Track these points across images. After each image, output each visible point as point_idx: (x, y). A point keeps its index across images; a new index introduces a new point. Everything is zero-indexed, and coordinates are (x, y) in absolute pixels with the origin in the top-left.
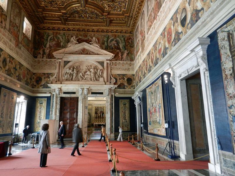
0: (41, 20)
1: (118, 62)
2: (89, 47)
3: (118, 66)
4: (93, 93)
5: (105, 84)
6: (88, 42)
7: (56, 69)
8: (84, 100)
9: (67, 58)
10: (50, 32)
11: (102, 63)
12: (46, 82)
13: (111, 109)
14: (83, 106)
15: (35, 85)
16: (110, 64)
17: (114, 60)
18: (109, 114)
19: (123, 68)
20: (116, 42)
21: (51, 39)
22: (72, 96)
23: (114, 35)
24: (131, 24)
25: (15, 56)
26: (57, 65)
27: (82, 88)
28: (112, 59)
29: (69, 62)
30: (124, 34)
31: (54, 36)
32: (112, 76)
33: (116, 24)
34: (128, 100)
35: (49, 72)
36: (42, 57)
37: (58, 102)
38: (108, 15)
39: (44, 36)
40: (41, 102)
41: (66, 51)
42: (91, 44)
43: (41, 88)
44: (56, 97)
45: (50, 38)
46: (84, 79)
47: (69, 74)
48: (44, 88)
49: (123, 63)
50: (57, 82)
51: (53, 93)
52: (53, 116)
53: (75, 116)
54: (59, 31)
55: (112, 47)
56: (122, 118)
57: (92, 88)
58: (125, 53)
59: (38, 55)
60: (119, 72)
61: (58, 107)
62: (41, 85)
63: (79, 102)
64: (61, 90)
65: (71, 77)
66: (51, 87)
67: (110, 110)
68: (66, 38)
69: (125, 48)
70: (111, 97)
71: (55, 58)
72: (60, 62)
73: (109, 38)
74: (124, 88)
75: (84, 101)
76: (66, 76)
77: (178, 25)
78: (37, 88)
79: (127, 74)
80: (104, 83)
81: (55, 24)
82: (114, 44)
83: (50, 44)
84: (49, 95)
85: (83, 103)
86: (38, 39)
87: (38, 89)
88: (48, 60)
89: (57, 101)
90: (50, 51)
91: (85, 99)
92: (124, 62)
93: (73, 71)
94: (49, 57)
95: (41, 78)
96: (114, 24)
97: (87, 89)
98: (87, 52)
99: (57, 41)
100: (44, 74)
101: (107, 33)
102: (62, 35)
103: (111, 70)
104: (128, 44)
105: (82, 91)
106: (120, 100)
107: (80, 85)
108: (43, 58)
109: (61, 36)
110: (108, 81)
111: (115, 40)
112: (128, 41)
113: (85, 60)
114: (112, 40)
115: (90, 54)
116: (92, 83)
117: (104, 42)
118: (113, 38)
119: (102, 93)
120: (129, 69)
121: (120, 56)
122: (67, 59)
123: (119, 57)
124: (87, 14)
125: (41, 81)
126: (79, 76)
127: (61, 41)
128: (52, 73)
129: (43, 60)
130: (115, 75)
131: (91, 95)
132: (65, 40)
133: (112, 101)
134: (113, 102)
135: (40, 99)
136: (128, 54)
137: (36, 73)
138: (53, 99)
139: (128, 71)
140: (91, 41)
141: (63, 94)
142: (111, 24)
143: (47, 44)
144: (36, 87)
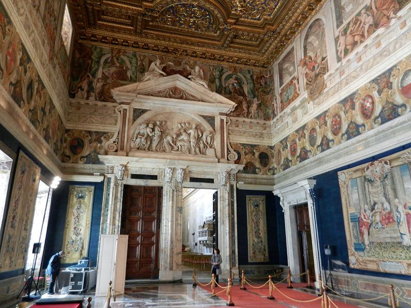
0: (92, 18)
1: (241, 119)
2: (187, 85)
3: (241, 129)
4: (193, 180)
5: (219, 162)
6: (186, 75)
7: (116, 124)
8: (175, 193)
9: (140, 102)
10: (106, 47)
11: (210, 120)
13: (231, 214)
14: (172, 207)
15: (69, 157)
16: (227, 123)
18: (227, 226)
19: (251, 132)
20: (236, 81)
21: (106, 62)
24: (270, 49)
29: (144, 111)
31: (112, 57)
32: (231, 147)
33: (240, 46)
34: (263, 197)
35: (101, 128)
36: (85, 96)
37: (119, 195)
38: (235, 24)
39: (92, 53)
40: (80, 195)
42: (189, 79)
43: (81, 162)
44: (115, 185)
45: (106, 60)
46: (176, 148)
47: (145, 136)
49: (251, 122)
51: (109, 176)
52: (106, 227)
53: (154, 228)
55: (230, 90)
56: (252, 234)
59: (78, 91)
60: (244, 140)
61: (119, 206)
65: (149, 143)
66: (105, 161)
67: (229, 217)
68: (139, 64)
71: (114, 101)
73: (224, 71)
74: (255, 173)
76: (138, 140)
78: (73, 163)
79: (258, 145)
81: (119, 32)
82: (233, 85)
83: (104, 71)
84: (99, 179)
85: (173, 201)
88: (100, 104)
89: (117, 193)
90: (104, 85)
91: (176, 191)
92: (253, 120)
93: (153, 130)
94: (102, 99)
95: (83, 142)
96: (237, 46)
100: (90, 133)
102: (131, 56)
103: (229, 134)
105: (172, 173)
106: (247, 197)
107: (168, 160)
108: (87, 98)
109: (128, 57)
110: (223, 156)
111: (234, 76)
112: (259, 81)
113: (177, 111)
114: (229, 77)
115: (186, 99)
116: (192, 158)
117: (215, 78)
118: (230, 73)
119: (211, 181)
120: (262, 134)
123: (244, 110)
124: (192, 18)
125: (82, 149)
127: (127, 67)
128: (108, 133)
129: (88, 104)
130: (237, 144)
131: (190, 183)
133: (232, 197)
134: (233, 199)
135: (78, 188)
136: (259, 106)
137: (72, 130)
138: (108, 190)
139: (262, 138)
140: (190, 74)
141: (129, 178)
143: (97, 70)
144: (71, 161)
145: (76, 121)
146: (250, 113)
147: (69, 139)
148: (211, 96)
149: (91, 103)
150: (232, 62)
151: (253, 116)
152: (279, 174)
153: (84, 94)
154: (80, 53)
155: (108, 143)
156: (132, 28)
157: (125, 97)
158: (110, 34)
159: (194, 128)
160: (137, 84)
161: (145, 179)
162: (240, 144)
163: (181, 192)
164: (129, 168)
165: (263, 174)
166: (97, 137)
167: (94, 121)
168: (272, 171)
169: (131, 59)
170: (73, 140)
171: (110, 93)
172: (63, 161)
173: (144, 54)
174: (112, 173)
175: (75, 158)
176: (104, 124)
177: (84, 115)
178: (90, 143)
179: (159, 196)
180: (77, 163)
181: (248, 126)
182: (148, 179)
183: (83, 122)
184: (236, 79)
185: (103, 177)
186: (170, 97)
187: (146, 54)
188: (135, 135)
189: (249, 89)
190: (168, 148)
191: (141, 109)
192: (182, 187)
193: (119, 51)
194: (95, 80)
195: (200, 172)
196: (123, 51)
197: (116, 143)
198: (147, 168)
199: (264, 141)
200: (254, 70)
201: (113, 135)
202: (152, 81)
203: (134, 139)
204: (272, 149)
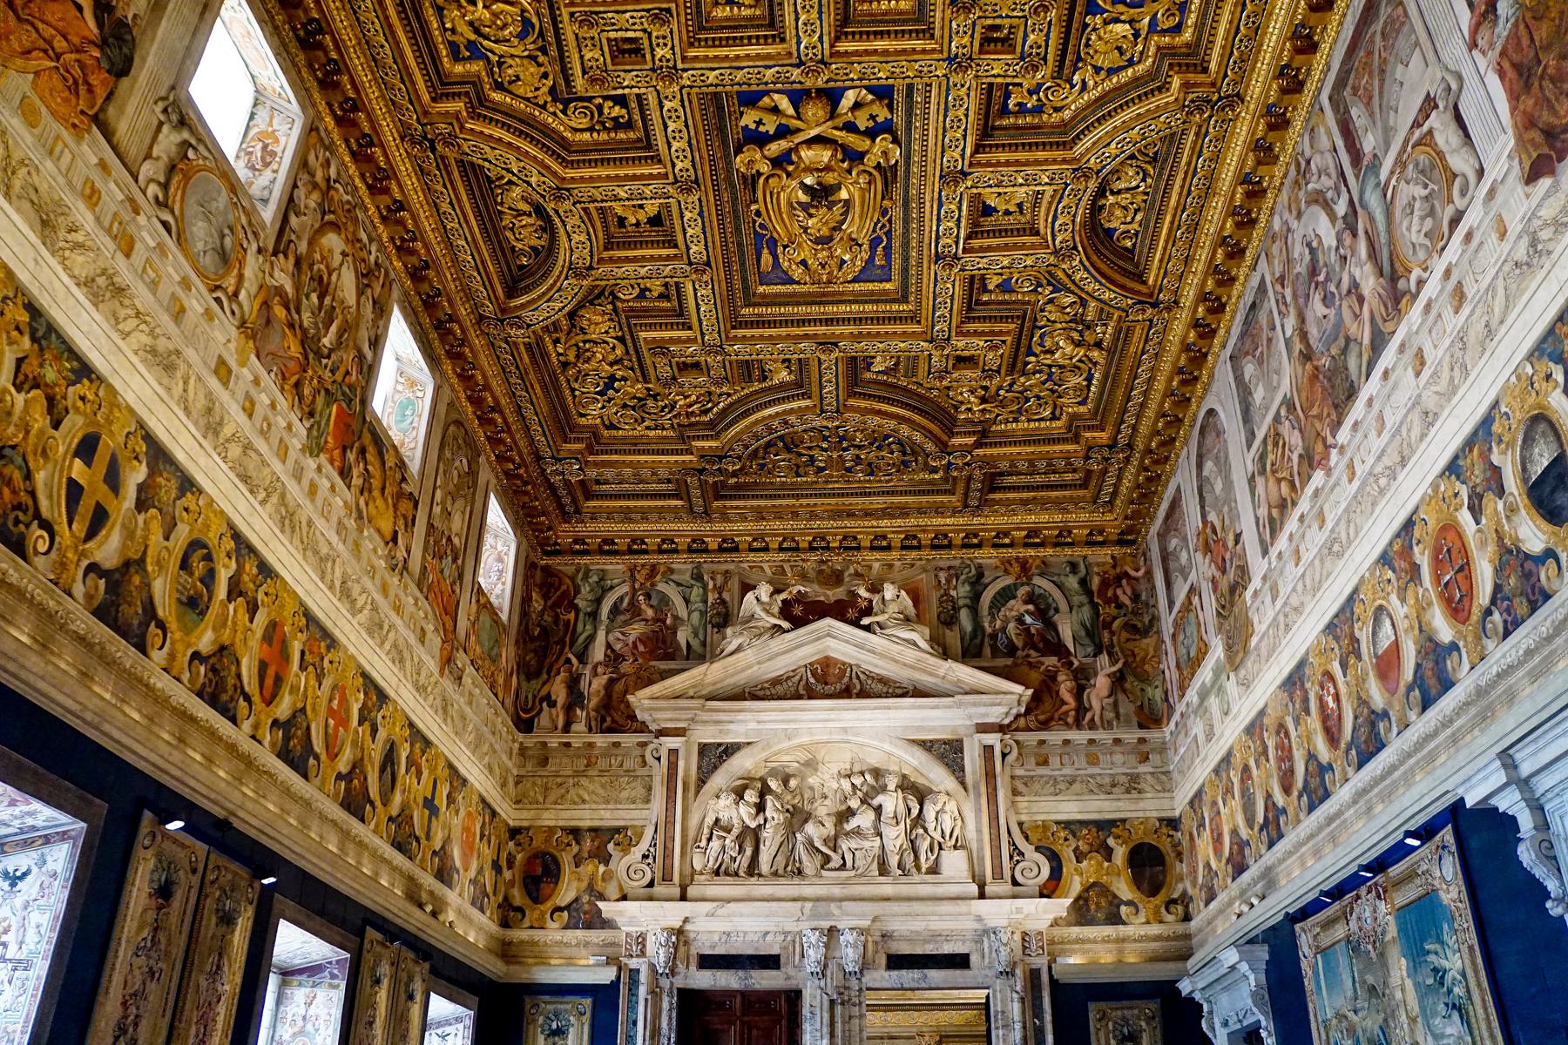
0: (567, 500)
1: (1055, 737)
2: (860, 646)
3: (1055, 769)
4: (897, 962)
5: (982, 896)
6: (852, 612)
7: (648, 801)
8: (838, 1009)
10: (616, 566)
11: (948, 752)
15: (520, 910)
16: (1004, 755)
17: (1028, 729)
19: (1092, 776)
20: (1031, 607)
21: (615, 610)
22: (757, 987)
23: (1017, 559)
24: (1123, 490)
25: (435, 728)
26: (659, 772)
27: (826, 924)
28: (1018, 716)
29: (730, 750)
30: (1079, 552)
31: (634, 591)
32: (1027, 838)
33: (1025, 495)
34: (1152, 1007)
35: (606, 817)
37: (664, 1024)
38: (978, 445)
39: (577, 591)
40: (554, 1026)
41: (709, 679)
42: (868, 628)
43: (555, 925)
44: (652, 992)
46: (836, 861)
47: (735, 832)
49: (1092, 742)
50: (658, 889)
51: (633, 963)
54: (663, 559)
55: (1011, 641)
57: (898, 926)
58: (1096, 675)
59: (541, 710)
60: (1070, 808)
62: (559, 909)
63: (807, 1027)
64: (686, 943)
65: (749, 852)
66: (619, 920)
68: (710, 600)
70: (1025, 987)
71: (643, 728)
72: (674, 753)
73: (986, 580)
74: (1115, 919)
75: (838, 1019)
76: (715, 844)
77: (1512, 510)
78: (532, 927)
79: (1124, 821)
80: (974, 889)
81: (645, 519)
82: (1020, 620)
83: (611, 638)
84: (606, 976)
85: (832, 1035)
86: (542, 612)
87: (541, 932)
88: (601, 740)
89: (657, 1016)
90: (611, 682)
91: (843, 1004)
92: (1099, 735)
93: (760, 808)
96: (1011, 495)
97: (862, 931)
98: (846, 680)
99: (656, 620)
100: (575, 832)
101: (967, 554)
103: (1015, 792)
105: (827, 946)
107: (809, 905)
108: (567, 729)
109: (679, 584)
110: (998, 875)
111: (1022, 591)
112: (1110, 594)
113: (836, 737)
114: (1006, 595)
116: (888, 890)
117: (956, 609)
118: (1008, 581)
119: (959, 961)
120: (1134, 778)
121: (1066, 695)
122: (712, 729)
123: (1064, 703)
124: (845, 450)
125: (556, 883)
126: (800, 848)
127: (676, 618)
128: (626, 828)
129: (568, 745)
130: (1045, 826)
131: (886, 974)
132: (703, 613)
133: (1037, 1012)
134: (1042, 1020)
135: (549, 1005)
136: (1118, 681)
137: (528, 829)
138: (632, 1007)
139: (1134, 795)
140: (868, 611)
141: (693, 968)
142: (991, 496)
143: (591, 638)
144: (527, 923)
146: (1086, 710)
147: (519, 857)
148: (941, 672)
149: (576, 742)
154: (546, 597)
156: (679, 503)
157: (669, 715)
159: (892, 786)
161: (743, 968)
162: (1058, 823)
164: (692, 936)
165: (1148, 922)
167: (586, 797)
168: (1180, 908)
171: (628, 705)
172: (505, 924)
173: (725, 567)
174: (643, 954)
175: (536, 914)
177: (559, 780)
178: (577, 866)
179: (789, 1021)
181: (1083, 759)
184: (1030, 599)
185: (615, 969)
187: (731, 567)
188: (706, 831)
189: (1077, 627)
190: (809, 864)
191: (720, 745)
192: (860, 990)
194: (587, 671)
196: (662, 569)
197: (650, 860)
198: (745, 933)
199: (1142, 805)
200: (1091, 559)
201: (640, 836)
203: (703, 844)
204: (1176, 829)
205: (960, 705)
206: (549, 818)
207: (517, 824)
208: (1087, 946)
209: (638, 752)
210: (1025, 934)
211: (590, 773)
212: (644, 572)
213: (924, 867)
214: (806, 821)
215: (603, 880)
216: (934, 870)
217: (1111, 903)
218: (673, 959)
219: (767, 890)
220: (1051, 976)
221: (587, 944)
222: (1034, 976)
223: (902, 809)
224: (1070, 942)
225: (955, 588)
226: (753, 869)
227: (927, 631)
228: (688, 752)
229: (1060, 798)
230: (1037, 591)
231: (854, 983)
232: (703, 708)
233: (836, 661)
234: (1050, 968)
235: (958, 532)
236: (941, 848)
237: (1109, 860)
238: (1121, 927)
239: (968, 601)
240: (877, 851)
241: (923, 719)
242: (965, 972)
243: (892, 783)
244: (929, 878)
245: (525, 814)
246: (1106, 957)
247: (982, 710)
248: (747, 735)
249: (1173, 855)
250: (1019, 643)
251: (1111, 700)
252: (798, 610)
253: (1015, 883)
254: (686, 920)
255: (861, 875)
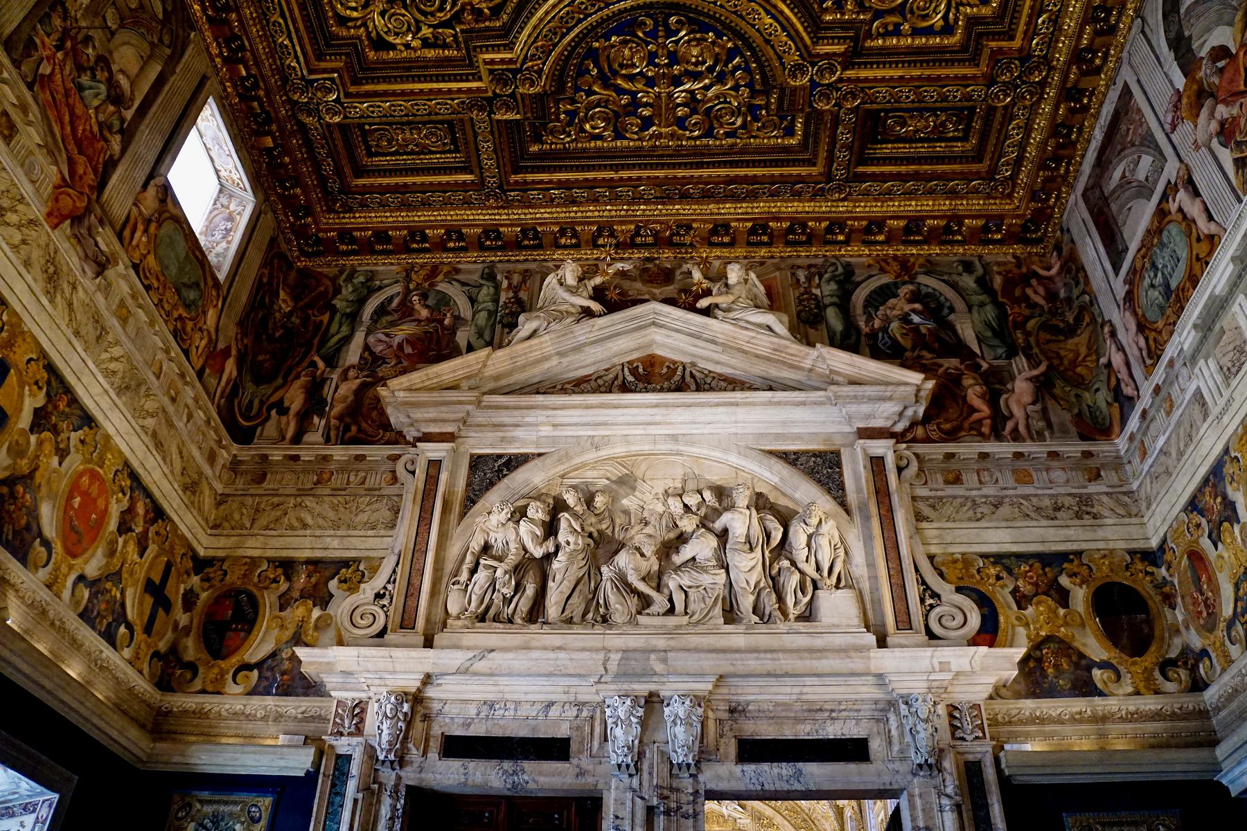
1: (967, 449)
3: (970, 487)
4: (752, 751)
7: (392, 525)
9: (498, 426)
10: (387, 267)
12: (288, 634)
15: (193, 668)
16: (900, 470)
17: (928, 440)
19: (1026, 497)
20: (917, 306)
21: (381, 311)
22: (532, 786)
23: (895, 257)
24: (1031, 152)
26: (413, 486)
27: (643, 688)
28: (913, 424)
29: (514, 463)
31: (407, 292)
32: (941, 575)
33: (903, 169)
35: (334, 546)
41: (490, 371)
42: (707, 312)
43: (238, 689)
44: (365, 789)
45: (382, 303)
46: (660, 603)
47: (512, 559)
48: (267, 693)
49: (1018, 455)
51: (343, 745)
54: (448, 258)
55: (894, 341)
57: (752, 693)
58: (1013, 379)
59: (268, 418)
62: (247, 667)
64: (427, 718)
65: (530, 590)
66: (330, 681)
69: (1003, 341)
70: (959, 787)
71: (398, 438)
72: (435, 465)
74: (1086, 688)
76: (482, 576)
78: (203, 692)
79: (1079, 554)
80: (871, 639)
83: (371, 339)
84: (298, 762)
86: (291, 313)
88: (340, 453)
91: (667, 813)
92: (1026, 447)
93: (551, 529)
95: (254, 604)
97: (698, 700)
98: (676, 378)
100: (287, 566)
101: (830, 251)
102: (475, 277)
103: (919, 517)
104: (1027, 312)
105: (644, 723)
108: (297, 439)
109: (464, 284)
110: (904, 622)
111: (905, 290)
113: (663, 447)
114: (883, 294)
117: (821, 307)
118: (886, 279)
119: (855, 750)
121: (977, 402)
122: (490, 435)
123: (974, 410)
124: (677, 81)
125: (249, 632)
126: (607, 586)
127: (457, 318)
128: (357, 561)
129: (296, 458)
130: (966, 560)
131: (738, 769)
132: (492, 314)
136: (1043, 387)
137: (223, 560)
139: (1088, 520)
141: (433, 755)
143: (347, 340)
144: (198, 684)
145: (242, 527)
147: (204, 596)
148: (807, 364)
150: (887, 242)
151: (1022, 428)
152: (1226, 678)
153: (288, 424)
154: (296, 298)
155: (354, 599)
156: (469, 177)
157: (431, 413)
158: (403, 217)
160: (482, 353)
162: (984, 556)
163: (695, 815)
164: (436, 706)
166: (313, 580)
167: (309, 520)
169: (476, 290)
170: (217, 601)
171: (378, 399)
172: (164, 684)
173: (521, 267)
174: (359, 731)
176: (349, 527)
177: (276, 500)
178: (282, 608)
180: (219, 693)
181: (1008, 474)
182: (527, 758)
183: (266, 528)
184: (915, 297)
186: (625, 388)
187: (533, 266)
188: (469, 558)
189: (981, 327)
190: (619, 607)
191: (500, 456)
192: (696, 793)
193: (434, 271)
195: (786, 706)
196: (445, 269)
197: (385, 602)
199: (1100, 533)
201: (374, 570)
202: (547, 337)
203: (464, 576)
205: (835, 401)
206: (254, 547)
207: (211, 553)
208: (1048, 728)
209: (389, 465)
210: (952, 708)
211: (319, 492)
212: (423, 273)
213: (793, 612)
214: (617, 552)
215: (316, 627)
216: (808, 615)
217: (1077, 665)
218: (402, 741)
219: (556, 640)
220: (999, 771)
221: (278, 718)
222: (972, 772)
223: (757, 531)
224: (1021, 722)
225: (819, 286)
226: (536, 613)
227: (785, 318)
228: (455, 465)
229: (983, 524)
230: (924, 290)
231: (687, 784)
232: (478, 404)
233: (663, 360)
234: (997, 761)
235: (819, 220)
236: (816, 587)
237: (1065, 605)
238: (1097, 700)
239: (835, 299)
240: (720, 590)
241: (784, 423)
242: (863, 766)
243: (742, 499)
244: (801, 626)
245: (222, 542)
246: (1082, 742)
247: (865, 408)
248: (538, 446)
249: (1158, 598)
250: (906, 343)
251: (1038, 407)
252: (613, 295)
253: (931, 635)
254: (428, 679)
255: (698, 622)
